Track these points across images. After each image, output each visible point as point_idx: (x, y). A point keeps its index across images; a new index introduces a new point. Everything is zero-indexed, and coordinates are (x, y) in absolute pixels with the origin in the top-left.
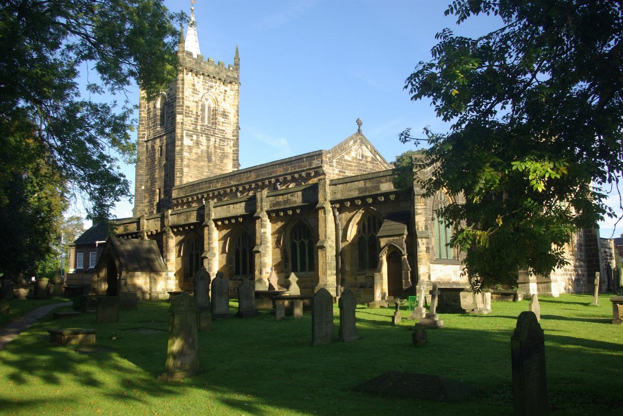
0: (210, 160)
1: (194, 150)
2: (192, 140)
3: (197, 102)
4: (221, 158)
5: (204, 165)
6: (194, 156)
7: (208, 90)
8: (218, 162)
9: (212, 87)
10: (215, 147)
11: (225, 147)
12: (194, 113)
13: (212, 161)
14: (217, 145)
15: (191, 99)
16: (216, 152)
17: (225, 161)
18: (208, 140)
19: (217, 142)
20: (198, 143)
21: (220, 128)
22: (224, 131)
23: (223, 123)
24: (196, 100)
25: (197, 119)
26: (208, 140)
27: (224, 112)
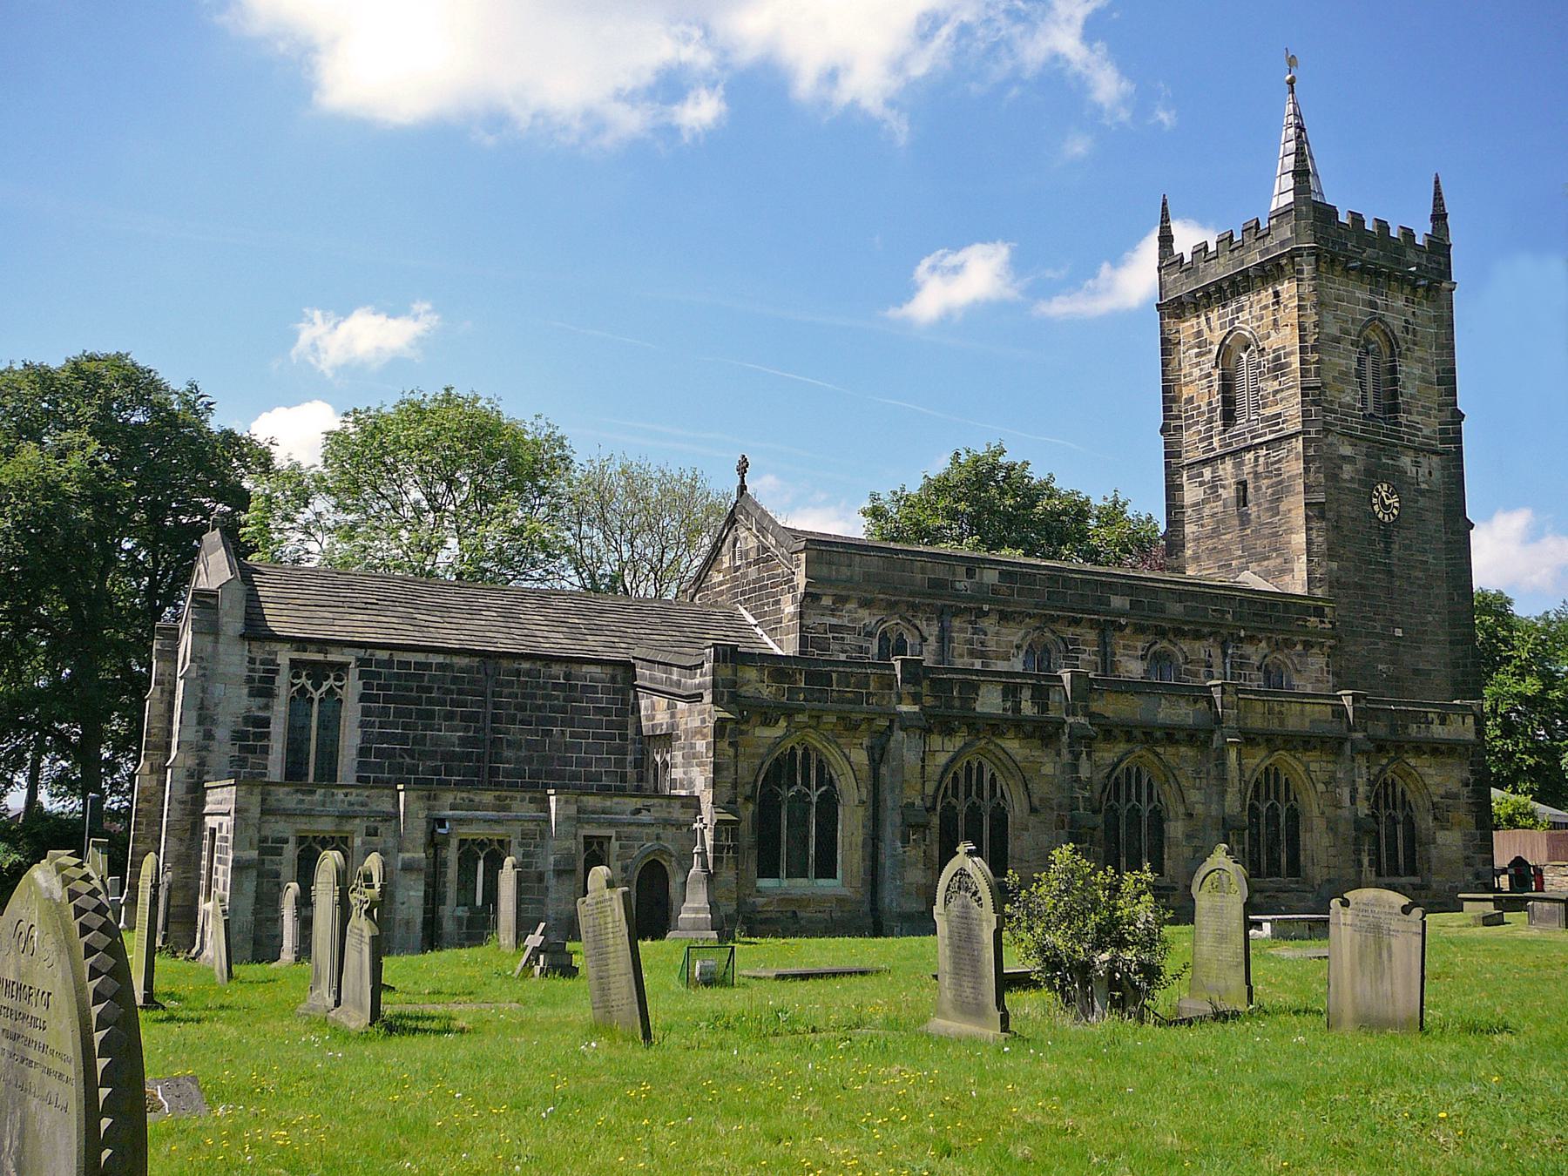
0: (1244, 520)
1: (1207, 511)
2: (1201, 484)
3: (1209, 375)
4: (1271, 502)
5: (1230, 541)
6: (1209, 524)
7: (1232, 322)
8: (1265, 519)
9: (1240, 309)
10: (1256, 475)
11: (1283, 465)
12: (1204, 408)
13: (1249, 521)
14: (1260, 469)
15: (1196, 372)
16: (1257, 489)
17: (1283, 507)
18: (1239, 465)
19: (1261, 460)
20: (1214, 486)
21: (1268, 412)
22: (1279, 415)
23: (1276, 392)
24: (1207, 367)
25: (1210, 421)
26: (1239, 465)
27: (1278, 358)
